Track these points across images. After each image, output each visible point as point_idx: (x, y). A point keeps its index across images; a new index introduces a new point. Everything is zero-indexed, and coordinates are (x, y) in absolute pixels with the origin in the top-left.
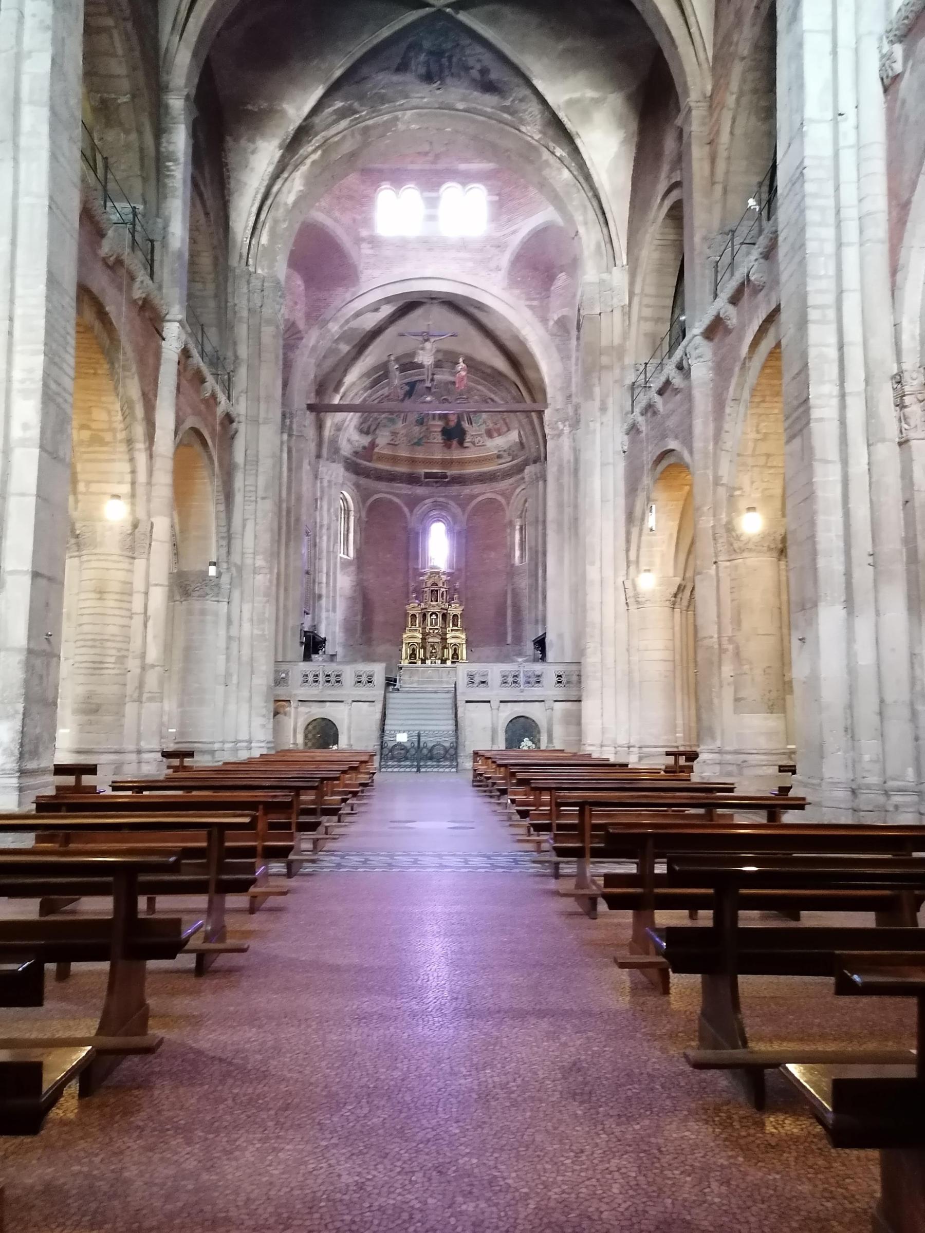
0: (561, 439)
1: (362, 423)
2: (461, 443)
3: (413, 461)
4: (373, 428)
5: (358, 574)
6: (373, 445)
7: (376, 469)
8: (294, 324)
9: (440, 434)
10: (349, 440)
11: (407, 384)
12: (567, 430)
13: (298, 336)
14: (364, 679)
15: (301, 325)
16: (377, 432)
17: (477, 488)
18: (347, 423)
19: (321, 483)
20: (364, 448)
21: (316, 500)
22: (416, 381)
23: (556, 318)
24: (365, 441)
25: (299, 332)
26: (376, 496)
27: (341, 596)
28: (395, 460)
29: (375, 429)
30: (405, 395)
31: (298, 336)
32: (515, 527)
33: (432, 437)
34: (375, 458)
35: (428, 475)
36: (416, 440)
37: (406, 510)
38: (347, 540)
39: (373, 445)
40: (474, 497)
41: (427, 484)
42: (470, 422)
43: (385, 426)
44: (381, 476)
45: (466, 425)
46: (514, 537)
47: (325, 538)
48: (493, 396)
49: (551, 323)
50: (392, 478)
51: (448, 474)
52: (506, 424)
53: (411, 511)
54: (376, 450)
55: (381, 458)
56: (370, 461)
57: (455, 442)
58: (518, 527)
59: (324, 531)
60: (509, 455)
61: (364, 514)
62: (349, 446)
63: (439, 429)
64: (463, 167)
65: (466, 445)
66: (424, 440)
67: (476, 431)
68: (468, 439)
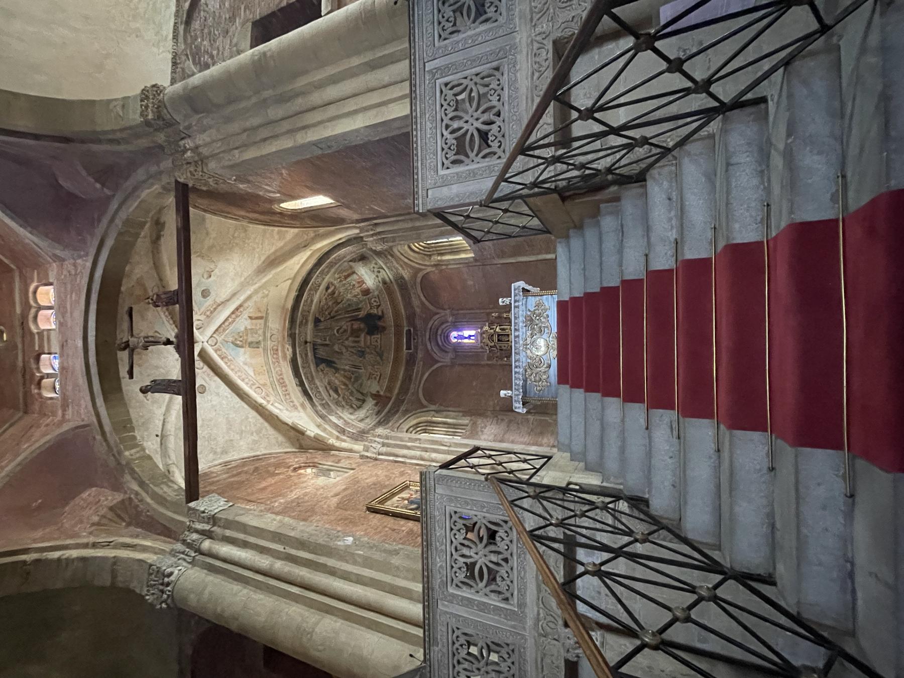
0: (205, 151)
1: (352, 407)
2: (380, 318)
3: (396, 360)
4: (361, 397)
5: (487, 417)
6: (376, 396)
7: (398, 394)
8: (111, 509)
9: (372, 337)
10: (362, 420)
11: (317, 365)
12: (189, 143)
13: (127, 503)
14: (481, 556)
15: (119, 497)
16: (365, 392)
17: (416, 302)
18: (340, 423)
19: (382, 454)
20: (376, 405)
21: (396, 462)
22: (315, 357)
23: (98, 186)
24: (370, 403)
25: (123, 501)
26: (421, 395)
27: (502, 441)
28: (393, 378)
29: (362, 394)
30: (331, 367)
31: (127, 503)
32: (439, 261)
33: (375, 344)
34: (389, 395)
35: (409, 348)
36: (378, 358)
37: (436, 366)
38: (454, 425)
39: (376, 396)
40: (422, 303)
41: (416, 348)
42: (358, 310)
43: (361, 385)
44: (404, 390)
45: (362, 314)
46: (448, 260)
47: (434, 455)
48: (322, 287)
49: (107, 192)
50: (408, 378)
51: (406, 329)
52: (349, 275)
53: (437, 362)
54: (382, 393)
55: (390, 389)
56: (390, 398)
57: (380, 323)
58: (439, 258)
59: (426, 455)
60: (379, 272)
61: (433, 407)
62: (368, 420)
63: (369, 337)
64: (18, 310)
65: (380, 313)
66: (378, 350)
67: (366, 304)
68: (375, 311)
